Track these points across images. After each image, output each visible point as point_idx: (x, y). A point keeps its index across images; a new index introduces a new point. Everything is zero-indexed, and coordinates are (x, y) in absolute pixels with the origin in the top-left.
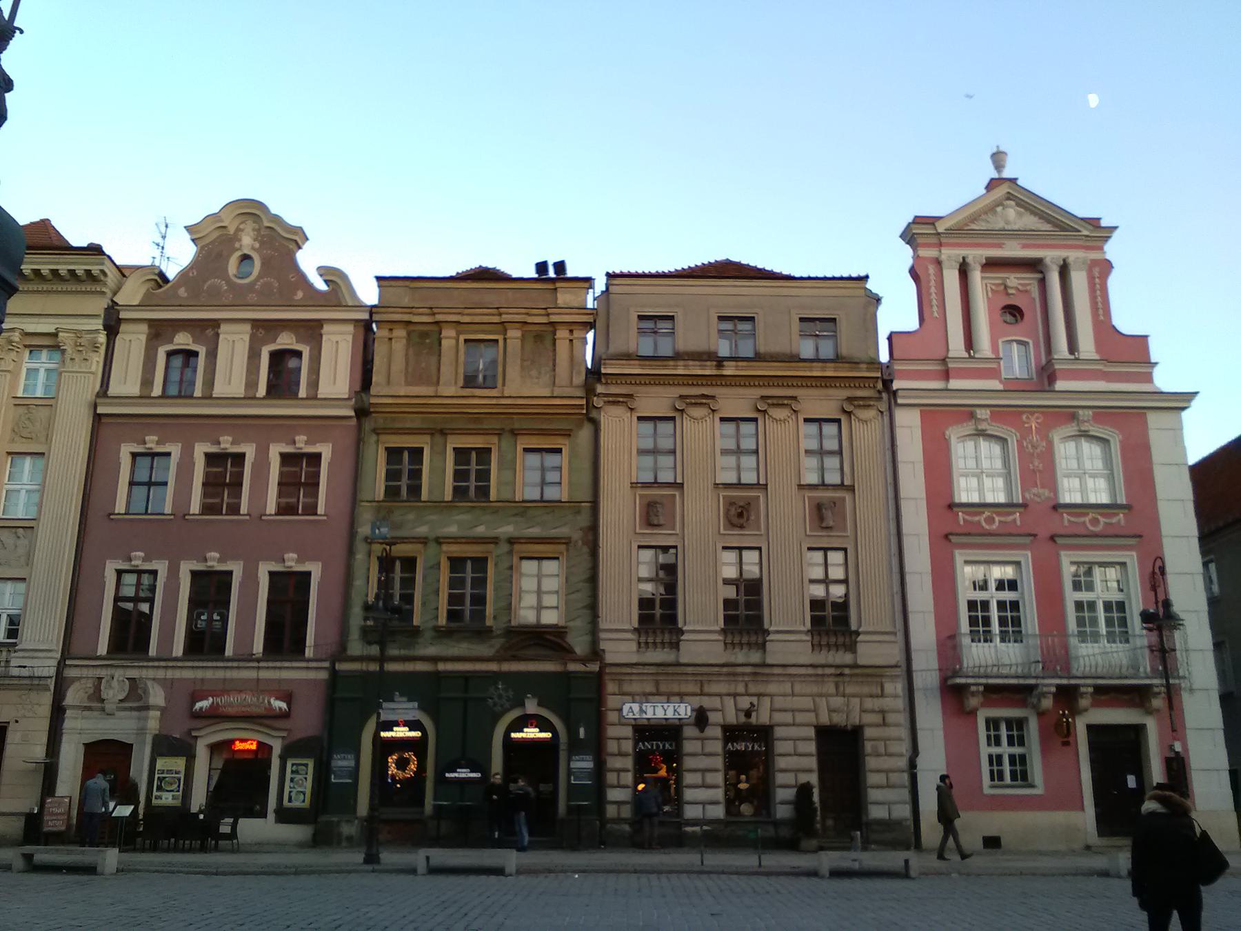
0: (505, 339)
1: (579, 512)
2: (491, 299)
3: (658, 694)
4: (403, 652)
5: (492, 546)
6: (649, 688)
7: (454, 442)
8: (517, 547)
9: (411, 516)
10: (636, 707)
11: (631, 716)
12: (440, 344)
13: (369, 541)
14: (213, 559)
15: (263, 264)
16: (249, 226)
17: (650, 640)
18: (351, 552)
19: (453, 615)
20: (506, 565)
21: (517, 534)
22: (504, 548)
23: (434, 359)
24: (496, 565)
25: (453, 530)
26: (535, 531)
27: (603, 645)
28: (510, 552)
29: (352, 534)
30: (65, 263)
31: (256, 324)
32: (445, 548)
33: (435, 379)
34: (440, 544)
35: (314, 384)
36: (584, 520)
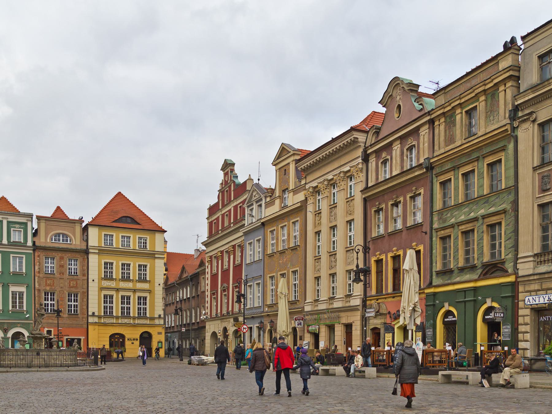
1: (510, 193)
3: (543, 290)
5: (476, 222)
6: (536, 287)
8: (486, 220)
9: (449, 215)
10: (531, 298)
11: (529, 303)
13: (437, 230)
17: (542, 259)
19: (467, 260)
20: (481, 231)
21: (485, 213)
22: (481, 221)
24: (478, 232)
25: (463, 218)
26: (493, 210)
27: (519, 266)
28: (482, 224)
29: (431, 228)
34: (458, 226)
36: (511, 198)
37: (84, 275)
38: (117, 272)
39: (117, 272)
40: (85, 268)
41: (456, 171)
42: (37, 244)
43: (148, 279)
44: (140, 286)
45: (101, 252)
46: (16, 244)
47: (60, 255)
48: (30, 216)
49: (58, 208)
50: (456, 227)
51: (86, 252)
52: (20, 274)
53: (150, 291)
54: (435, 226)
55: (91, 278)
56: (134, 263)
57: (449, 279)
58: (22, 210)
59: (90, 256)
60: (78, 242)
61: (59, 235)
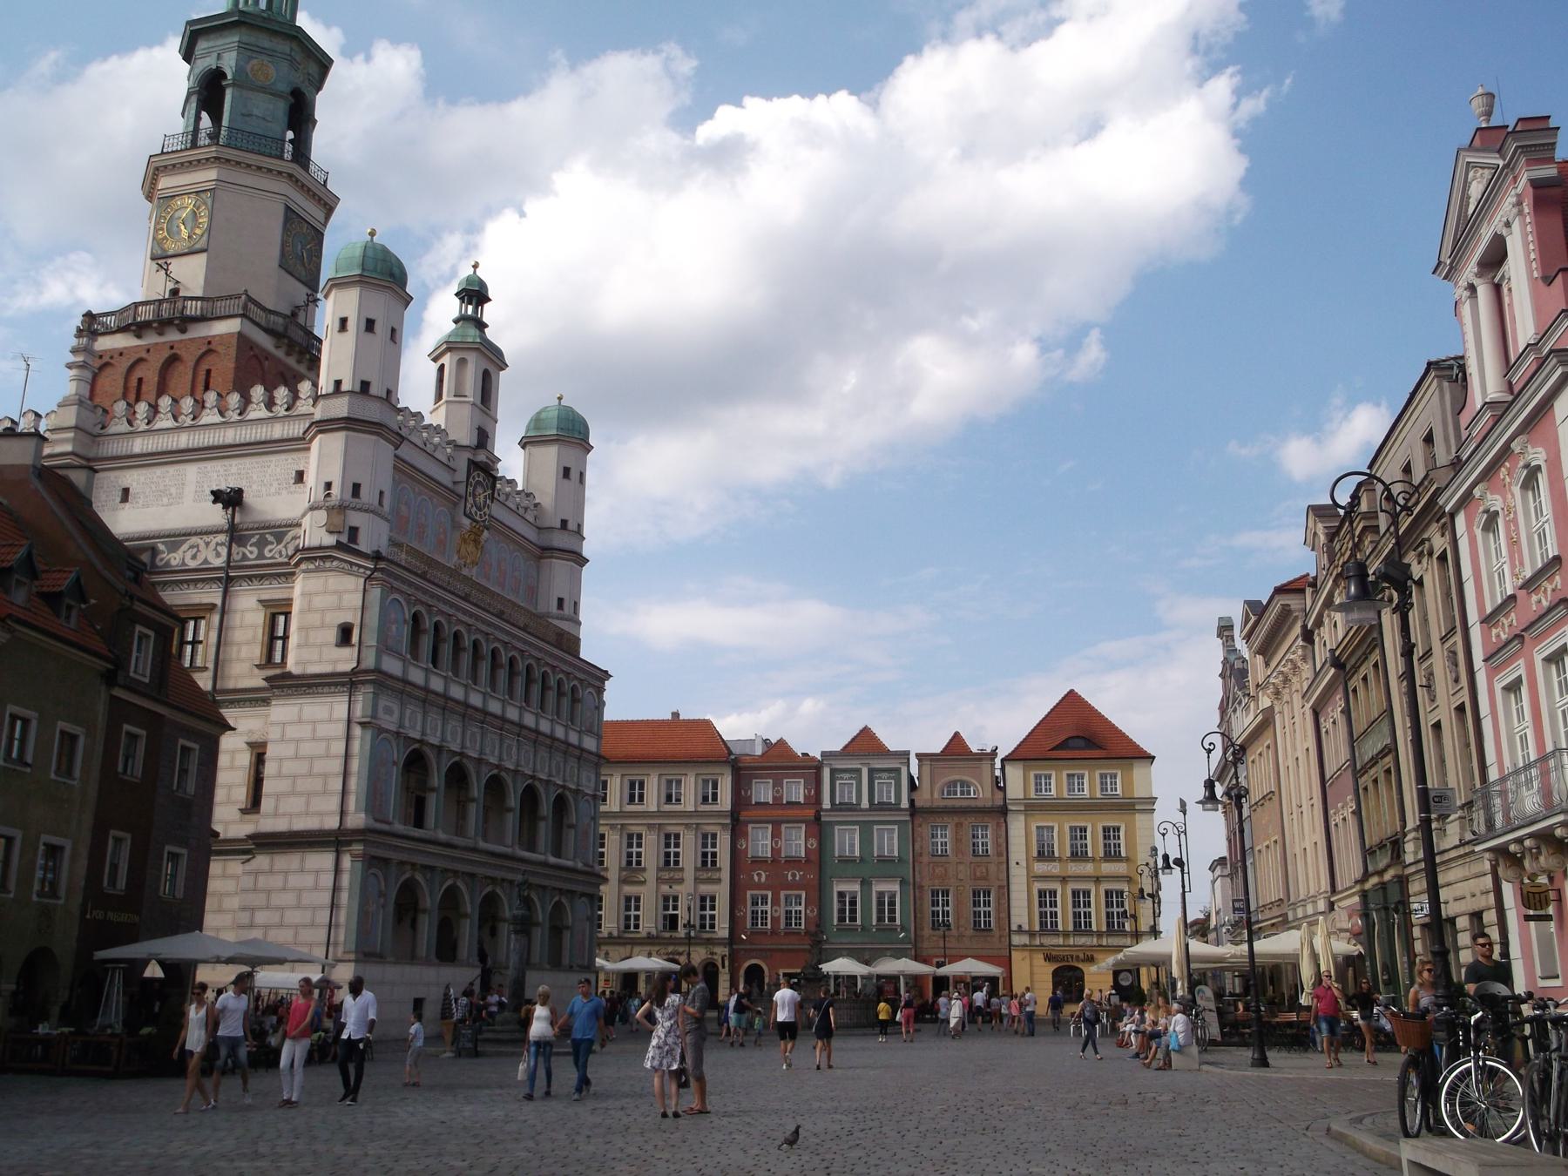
37: (999, 854)
38: (1061, 844)
39: (1061, 844)
40: (1002, 840)
42: (918, 804)
43: (1123, 854)
44: (1108, 868)
45: (1031, 808)
46: (883, 807)
47: (956, 819)
48: (905, 755)
49: (957, 735)
51: (1003, 811)
52: (890, 860)
53: (1129, 880)
55: (1013, 858)
56: (1094, 827)
58: (892, 745)
59: (1010, 817)
60: (989, 795)
61: (954, 783)
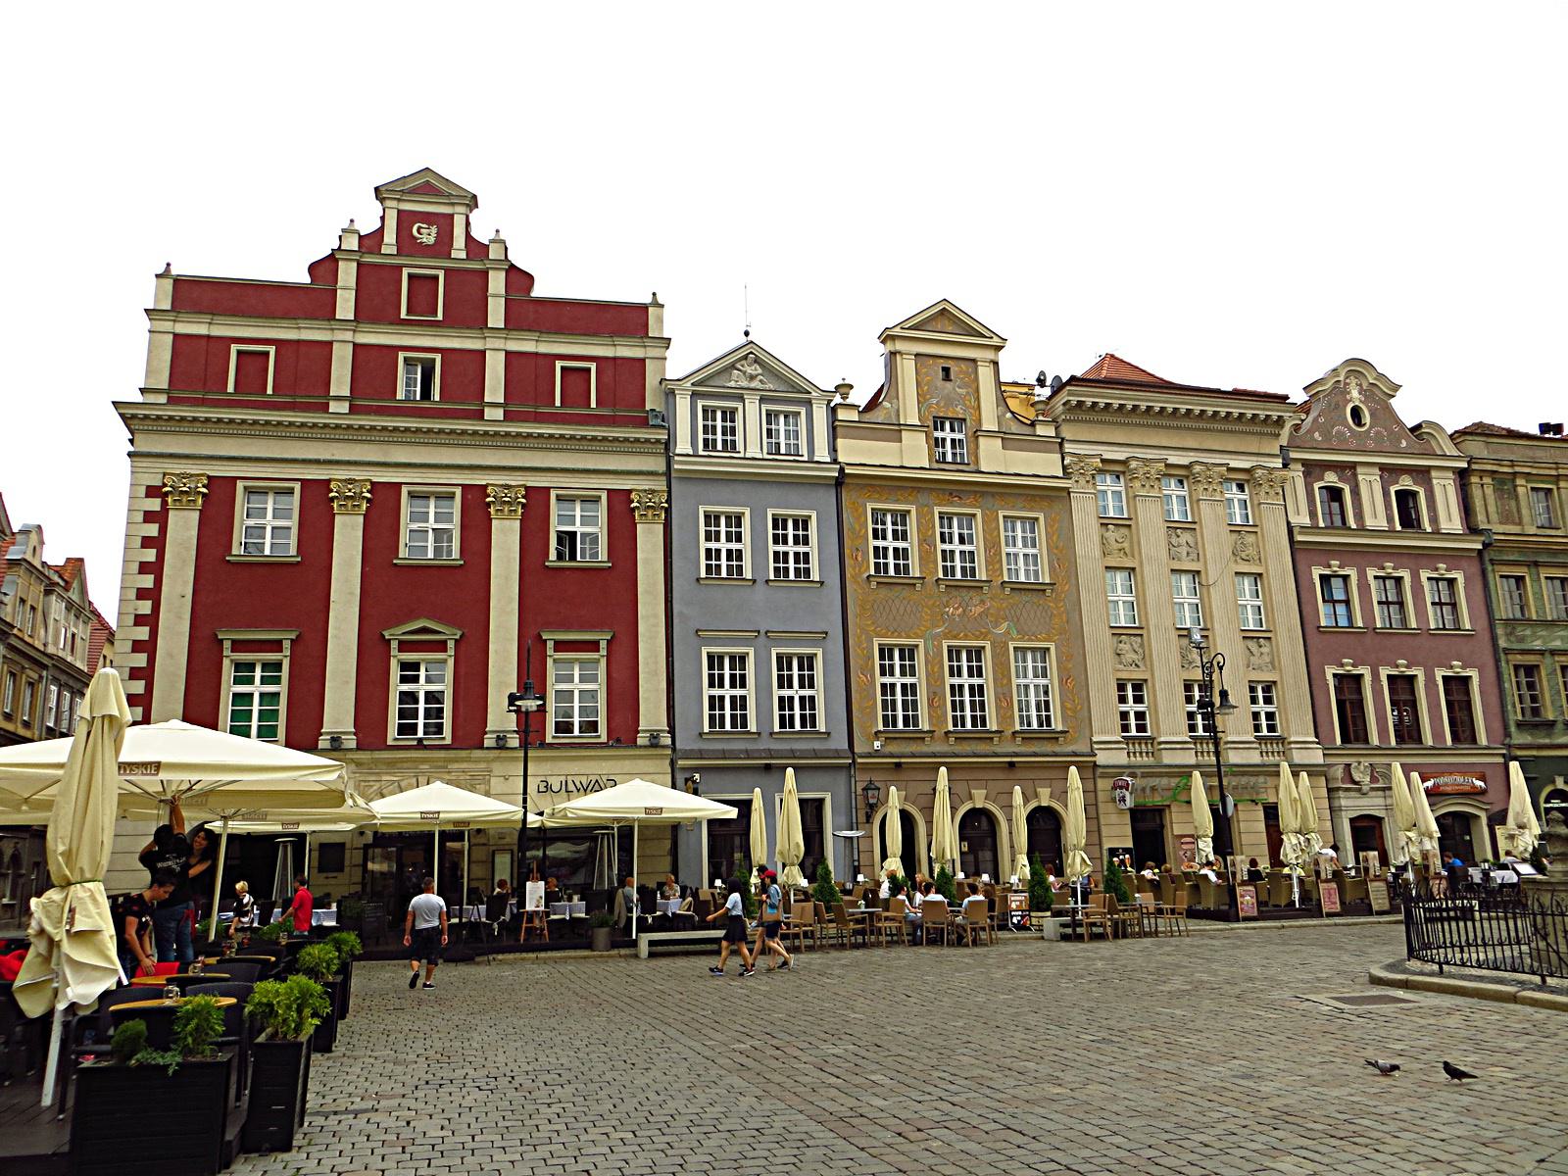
0: (1558, 488)
2: (1540, 454)
4: (1547, 741)
7: (1544, 573)
9: (1528, 632)
12: (1515, 490)
14: (1347, 664)
15: (1371, 415)
16: (1353, 381)
18: (1497, 661)
23: (1513, 503)
30: (1264, 409)
31: (1383, 468)
32: (1557, 658)
33: (1517, 520)
35: (1434, 520)
41: (1533, 570)
50: (1547, 655)
54: (1502, 643)
57: (1549, 736)
